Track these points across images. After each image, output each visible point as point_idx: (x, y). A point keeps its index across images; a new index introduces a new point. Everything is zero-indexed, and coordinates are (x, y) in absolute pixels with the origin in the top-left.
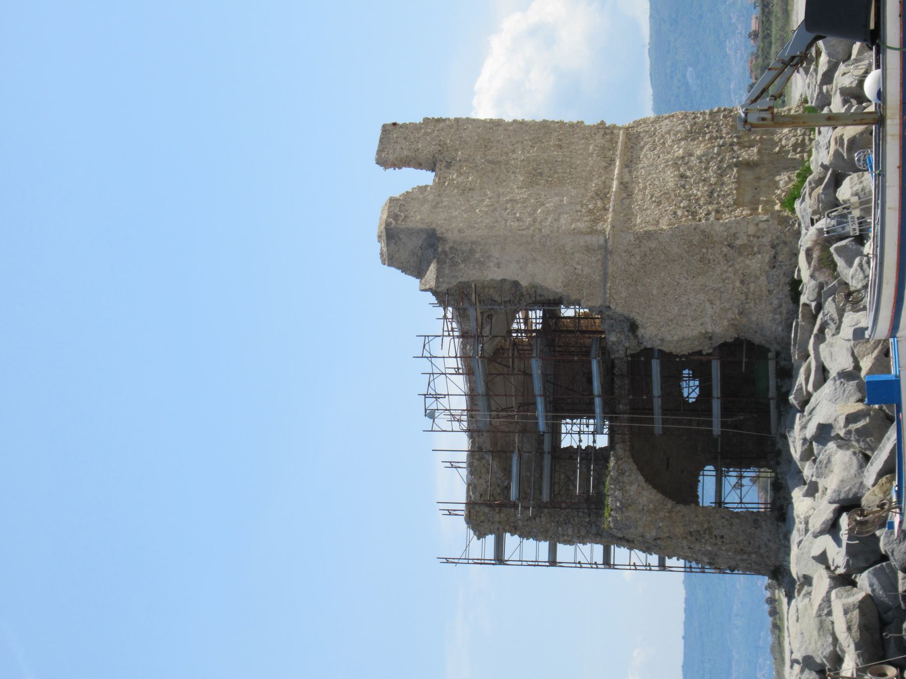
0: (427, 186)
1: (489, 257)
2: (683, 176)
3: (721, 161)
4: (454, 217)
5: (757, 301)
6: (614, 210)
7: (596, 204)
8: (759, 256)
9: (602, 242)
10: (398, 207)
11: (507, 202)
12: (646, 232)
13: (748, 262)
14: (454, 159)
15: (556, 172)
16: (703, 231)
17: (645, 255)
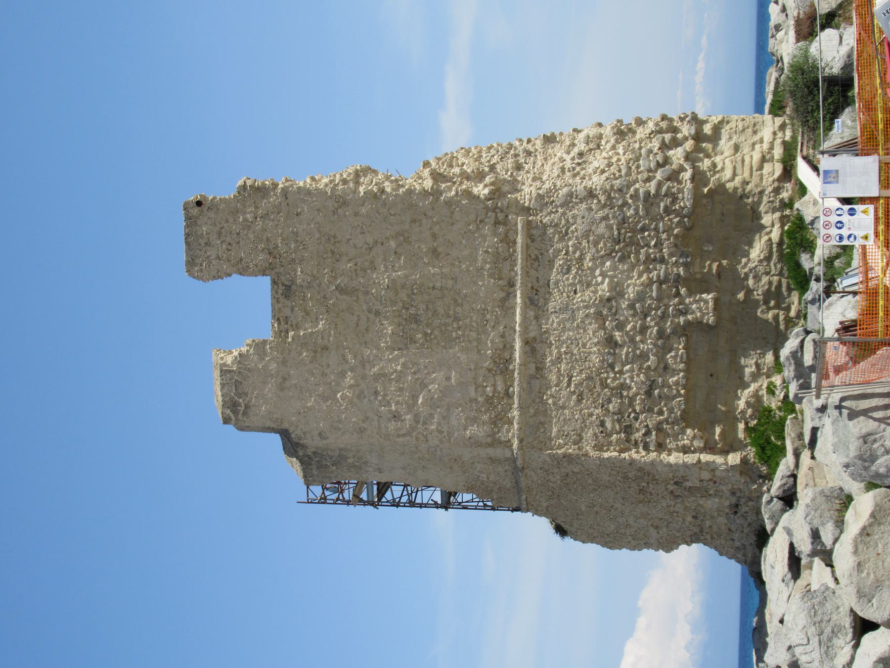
0: (265, 342)
1: (365, 463)
2: (610, 341)
3: (664, 317)
4: (310, 409)
5: (715, 536)
6: (520, 407)
7: (494, 385)
8: (717, 500)
11: (377, 377)
12: (565, 456)
13: (701, 503)
14: (293, 282)
15: (435, 313)
16: (640, 469)
17: (567, 475)
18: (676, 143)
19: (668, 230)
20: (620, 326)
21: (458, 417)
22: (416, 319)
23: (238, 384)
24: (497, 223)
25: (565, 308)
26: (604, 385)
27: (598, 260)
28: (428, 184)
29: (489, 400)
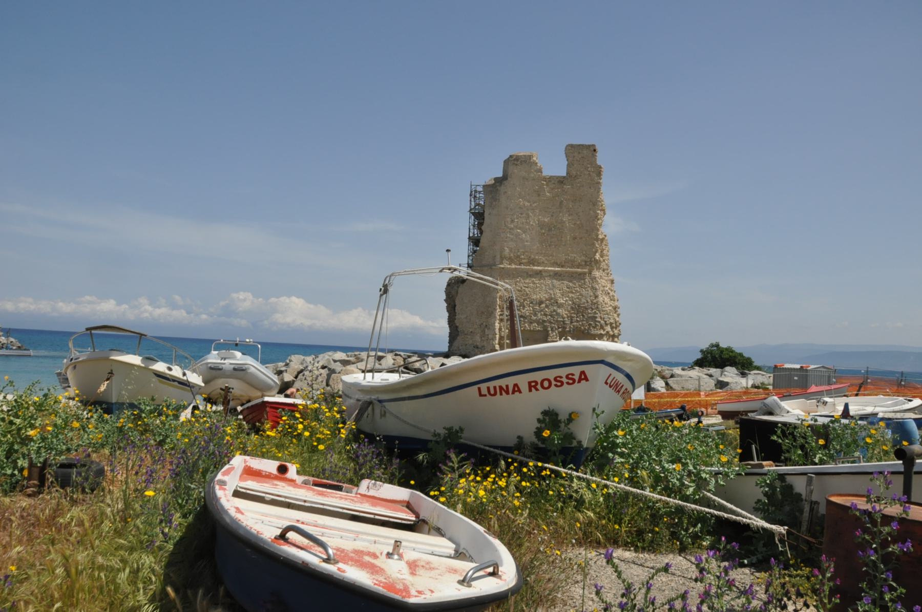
2: (541, 302)
3: (551, 323)
11: (528, 215)
18: (612, 328)
19: (583, 325)
20: (547, 306)
22: (550, 230)
23: (525, 162)
24: (586, 262)
25: (554, 286)
26: (524, 300)
27: (572, 299)
28: (600, 237)
29: (518, 257)
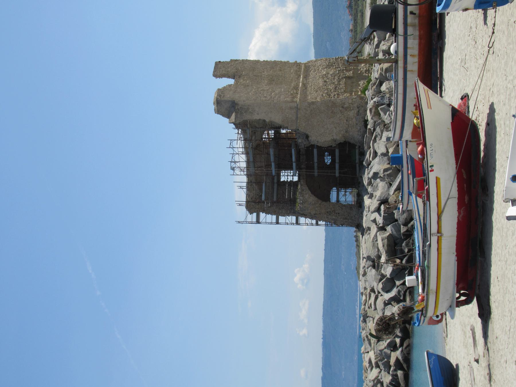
3: (339, 76)
9: (296, 105)
10: (221, 92)
11: (261, 90)
12: (312, 102)
14: (242, 75)
21: (282, 97)
